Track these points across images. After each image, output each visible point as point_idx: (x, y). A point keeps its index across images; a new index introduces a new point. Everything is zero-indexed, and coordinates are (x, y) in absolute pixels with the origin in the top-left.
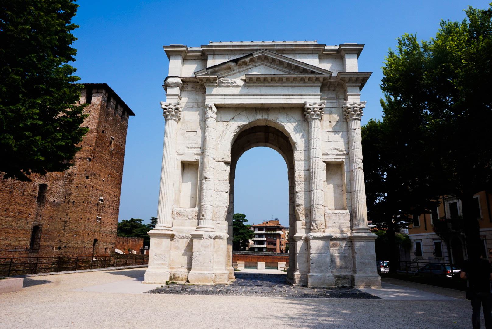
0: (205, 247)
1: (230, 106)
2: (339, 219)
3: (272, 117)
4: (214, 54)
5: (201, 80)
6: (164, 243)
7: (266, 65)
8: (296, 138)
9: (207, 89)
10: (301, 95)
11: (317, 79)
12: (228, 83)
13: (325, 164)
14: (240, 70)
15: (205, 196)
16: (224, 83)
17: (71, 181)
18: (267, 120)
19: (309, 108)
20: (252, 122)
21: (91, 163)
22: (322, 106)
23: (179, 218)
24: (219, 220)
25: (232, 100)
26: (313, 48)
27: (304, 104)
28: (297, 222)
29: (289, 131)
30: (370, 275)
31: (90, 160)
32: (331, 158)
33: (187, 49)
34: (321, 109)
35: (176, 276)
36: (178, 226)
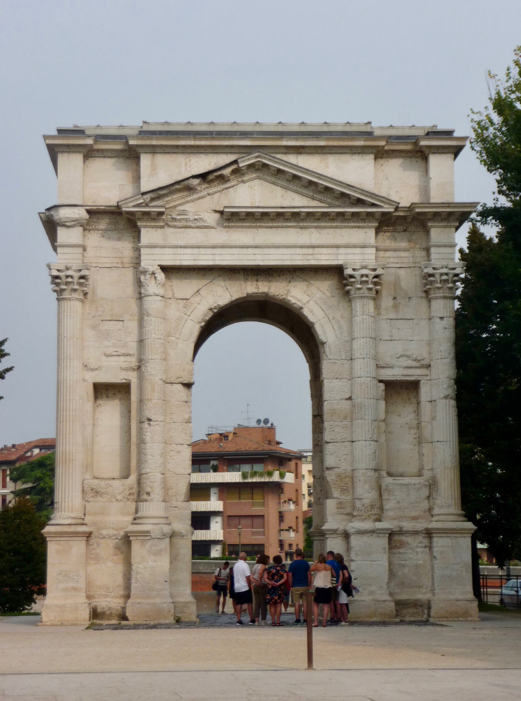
2: (408, 495)
4: (154, 153)
5: (132, 213)
7: (266, 181)
9: (143, 231)
10: (338, 247)
11: (370, 215)
12: (187, 220)
13: (382, 386)
14: (211, 191)
15: (149, 457)
18: (266, 294)
19: (351, 276)
24: (177, 500)
26: (361, 143)
30: (460, 597)
34: (376, 276)
35: (99, 610)
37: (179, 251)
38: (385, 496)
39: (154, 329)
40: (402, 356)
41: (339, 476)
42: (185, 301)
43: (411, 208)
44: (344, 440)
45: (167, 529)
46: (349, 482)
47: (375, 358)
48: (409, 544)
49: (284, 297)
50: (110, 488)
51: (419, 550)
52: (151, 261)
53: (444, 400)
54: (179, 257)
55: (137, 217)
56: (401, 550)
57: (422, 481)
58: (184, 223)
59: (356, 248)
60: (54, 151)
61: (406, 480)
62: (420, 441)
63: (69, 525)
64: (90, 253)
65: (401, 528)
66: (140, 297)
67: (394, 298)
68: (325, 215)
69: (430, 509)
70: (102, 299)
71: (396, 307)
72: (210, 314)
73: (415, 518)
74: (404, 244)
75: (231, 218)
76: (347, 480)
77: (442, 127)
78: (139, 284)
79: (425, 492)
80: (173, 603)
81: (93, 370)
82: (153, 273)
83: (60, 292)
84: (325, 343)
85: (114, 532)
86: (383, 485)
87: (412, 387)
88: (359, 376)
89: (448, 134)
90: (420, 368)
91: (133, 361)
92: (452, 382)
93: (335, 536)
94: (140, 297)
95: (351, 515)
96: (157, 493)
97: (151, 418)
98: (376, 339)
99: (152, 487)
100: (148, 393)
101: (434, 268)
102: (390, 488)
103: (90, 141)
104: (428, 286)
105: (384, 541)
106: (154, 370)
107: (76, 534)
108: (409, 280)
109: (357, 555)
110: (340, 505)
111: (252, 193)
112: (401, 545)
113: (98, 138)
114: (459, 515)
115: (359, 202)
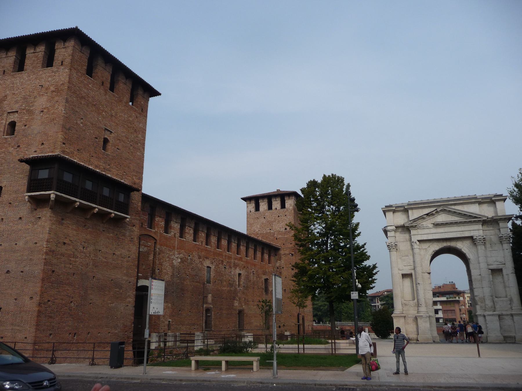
3: (453, 244)
13: (490, 271)
17: (280, 273)
21: (294, 257)
29: (465, 252)
31: (292, 255)
38: (496, 304)
39: (418, 258)
41: (480, 298)
43: (492, 218)
45: (427, 315)
46: (483, 300)
47: (487, 262)
52: (415, 239)
59: (476, 231)
60: (385, 212)
61: (501, 299)
62: (505, 287)
64: (397, 238)
66: (413, 249)
68: (465, 222)
69: (511, 308)
71: (491, 247)
73: (506, 311)
74: (491, 228)
75: (437, 225)
77: (498, 194)
78: (412, 246)
79: (509, 302)
83: (390, 249)
87: (500, 270)
89: (501, 195)
91: (412, 267)
94: (413, 249)
95: (485, 310)
96: (423, 305)
98: (486, 257)
100: (418, 276)
103: (394, 208)
104: (501, 240)
105: (497, 318)
106: (419, 269)
107: (401, 316)
108: (495, 239)
110: (481, 307)
111: (442, 218)
113: (396, 207)
115: (475, 217)
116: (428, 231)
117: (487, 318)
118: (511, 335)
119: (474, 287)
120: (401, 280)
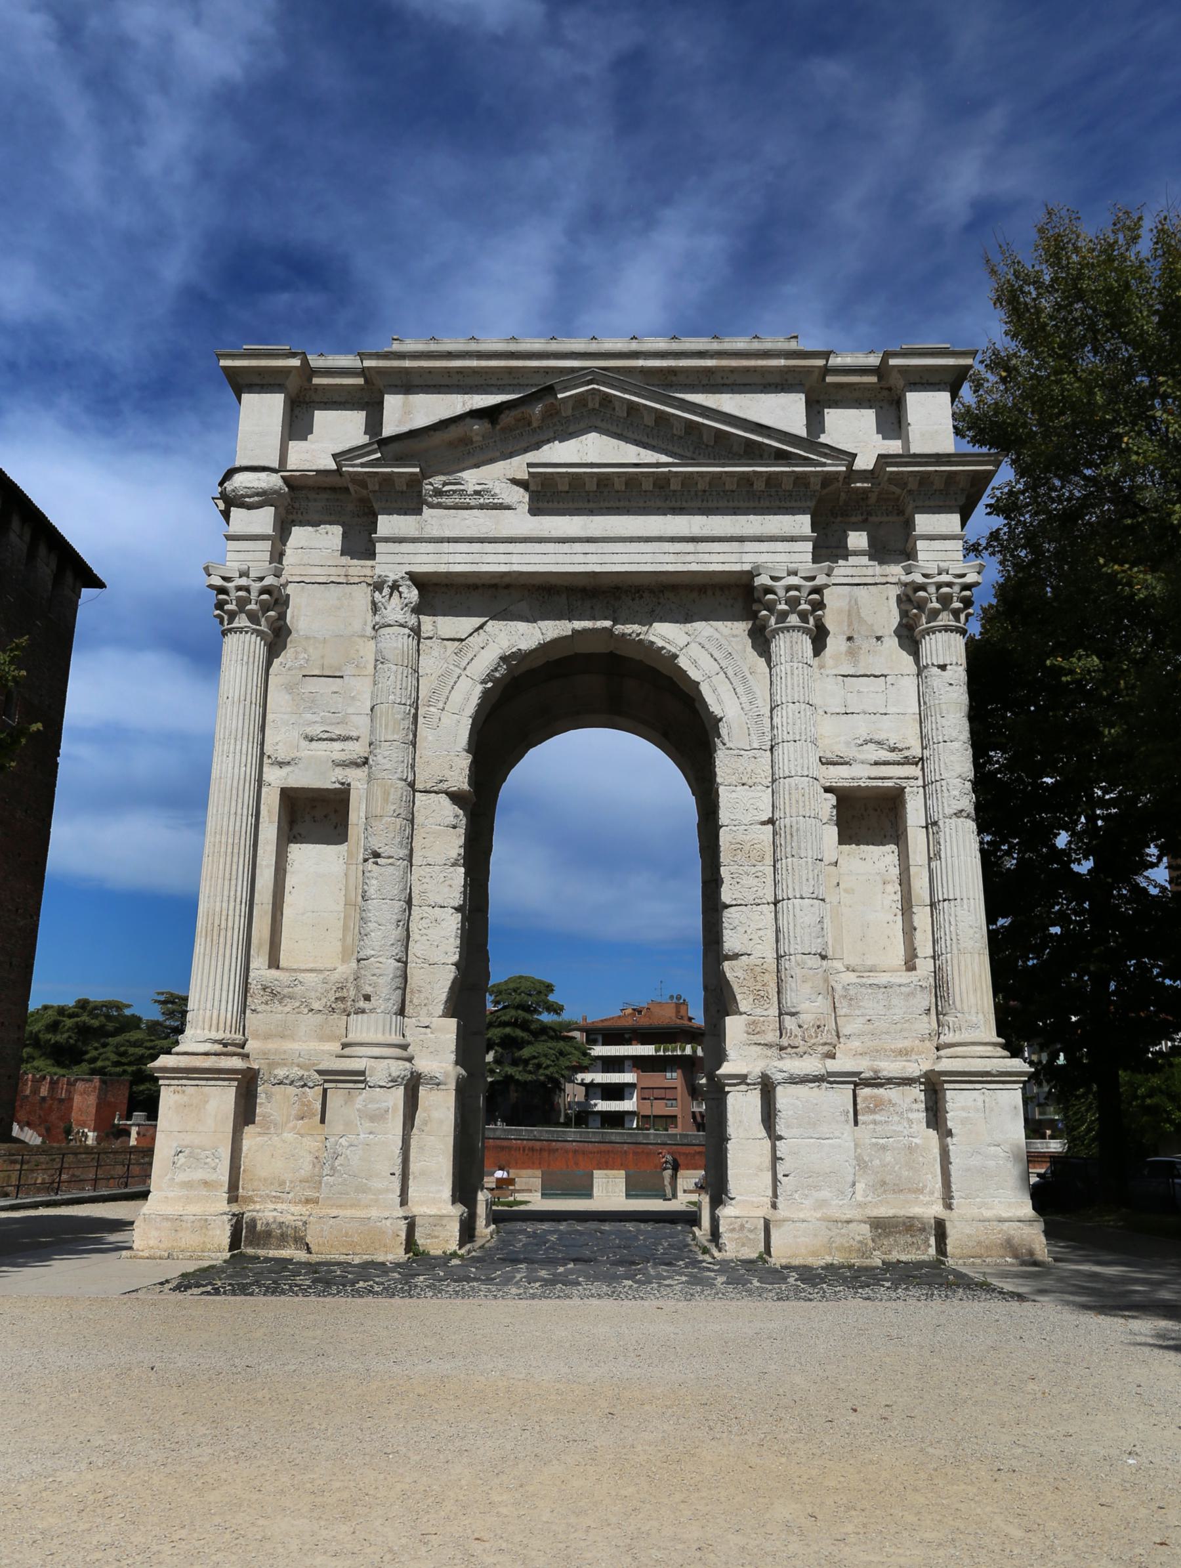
0: (372, 1119)
1: (471, 581)
6: (212, 1106)
8: (720, 702)
10: (741, 539)
11: (800, 478)
12: (462, 493)
13: (832, 799)
16: (447, 493)
19: (769, 590)
20: (555, 642)
22: (818, 582)
23: (277, 1007)
24: (430, 1015)
25: (477, 558)
27: (751, 575)
28: (729, 1020)
29: (694, 674)
32: (857, 775)
33: (305, 362)
36: (268, 1037)
37: (445, 547)
40: (866, 742)
41: (750, 969)
42: (457, 643)
44: (759, 901)
48: (894, 1105)
49: (641, 637)
50: (300, 987)
51: (912, 1116)
53: (954, 819)
54: (445, 558)
55: (370, 487)
56: (877, 1117)
57: (915, 979)
58: (457, 499)
63: (206, 1054)
65: (875, 1072)
67: (850, 639)
70: (307, 638)
71: (852, 654)
72: (503, 669)
73: (904, 1053)
76: (767, 977)
79: (926, 1000)
80: (406, 1218)
81: (281, 764)
82: (395, 587)
84: (721, 719)
85: (300, 1073)
86: (838, 987)
88: (787, 774)
90: (903, 764)
92: (968, 785)
93: (743, 1087)
97: (379, 851)
99: (374, 985)
101: (925, 576)
102: (851, 992)
109: (788, 1127)
110: (753, 1029)
112: (876, 1106)
114: (995, 1044)
116: (489, 523)
117: (785, 1097)
118: (916, 1210)
119: (726, 896)
120: (269, 832)
